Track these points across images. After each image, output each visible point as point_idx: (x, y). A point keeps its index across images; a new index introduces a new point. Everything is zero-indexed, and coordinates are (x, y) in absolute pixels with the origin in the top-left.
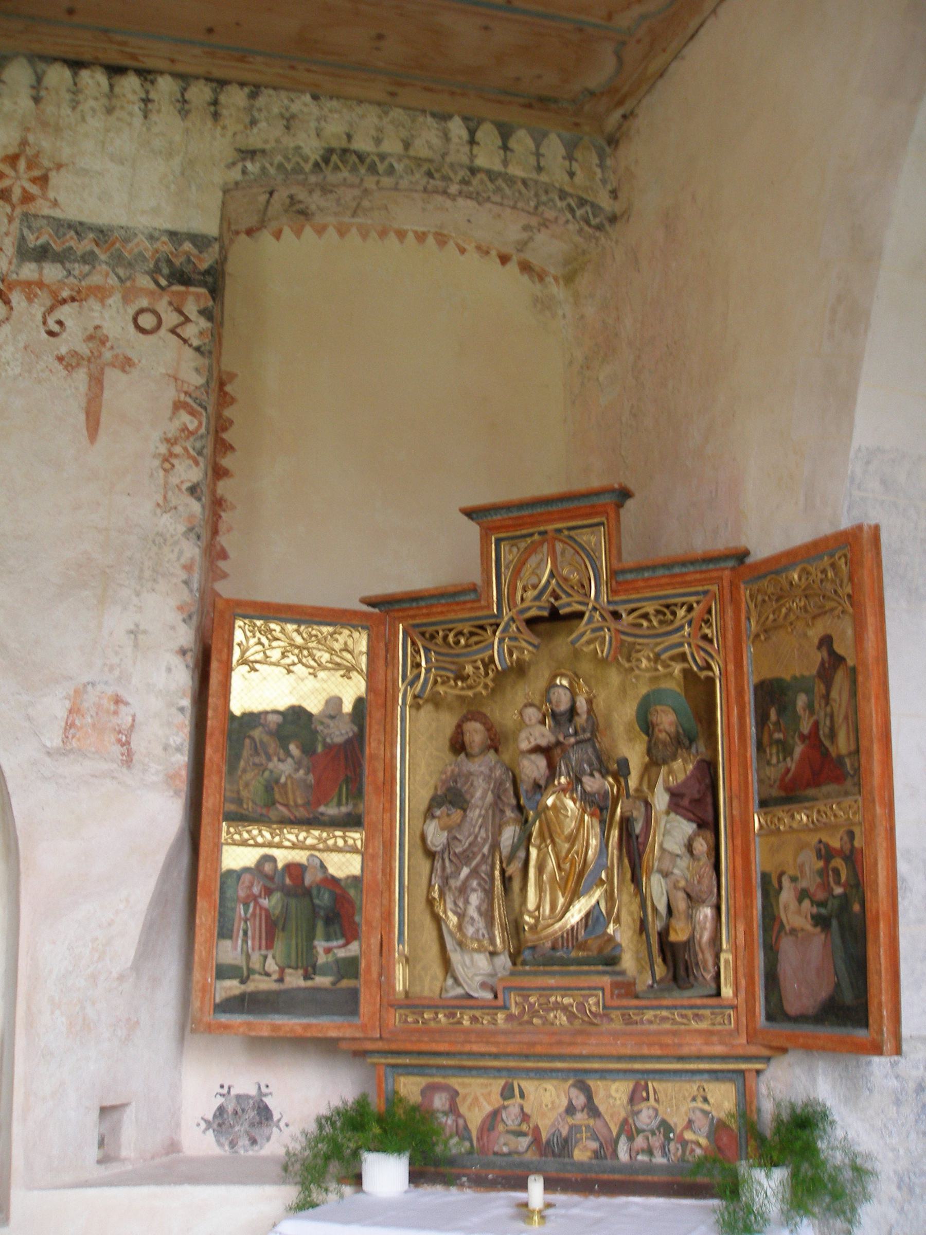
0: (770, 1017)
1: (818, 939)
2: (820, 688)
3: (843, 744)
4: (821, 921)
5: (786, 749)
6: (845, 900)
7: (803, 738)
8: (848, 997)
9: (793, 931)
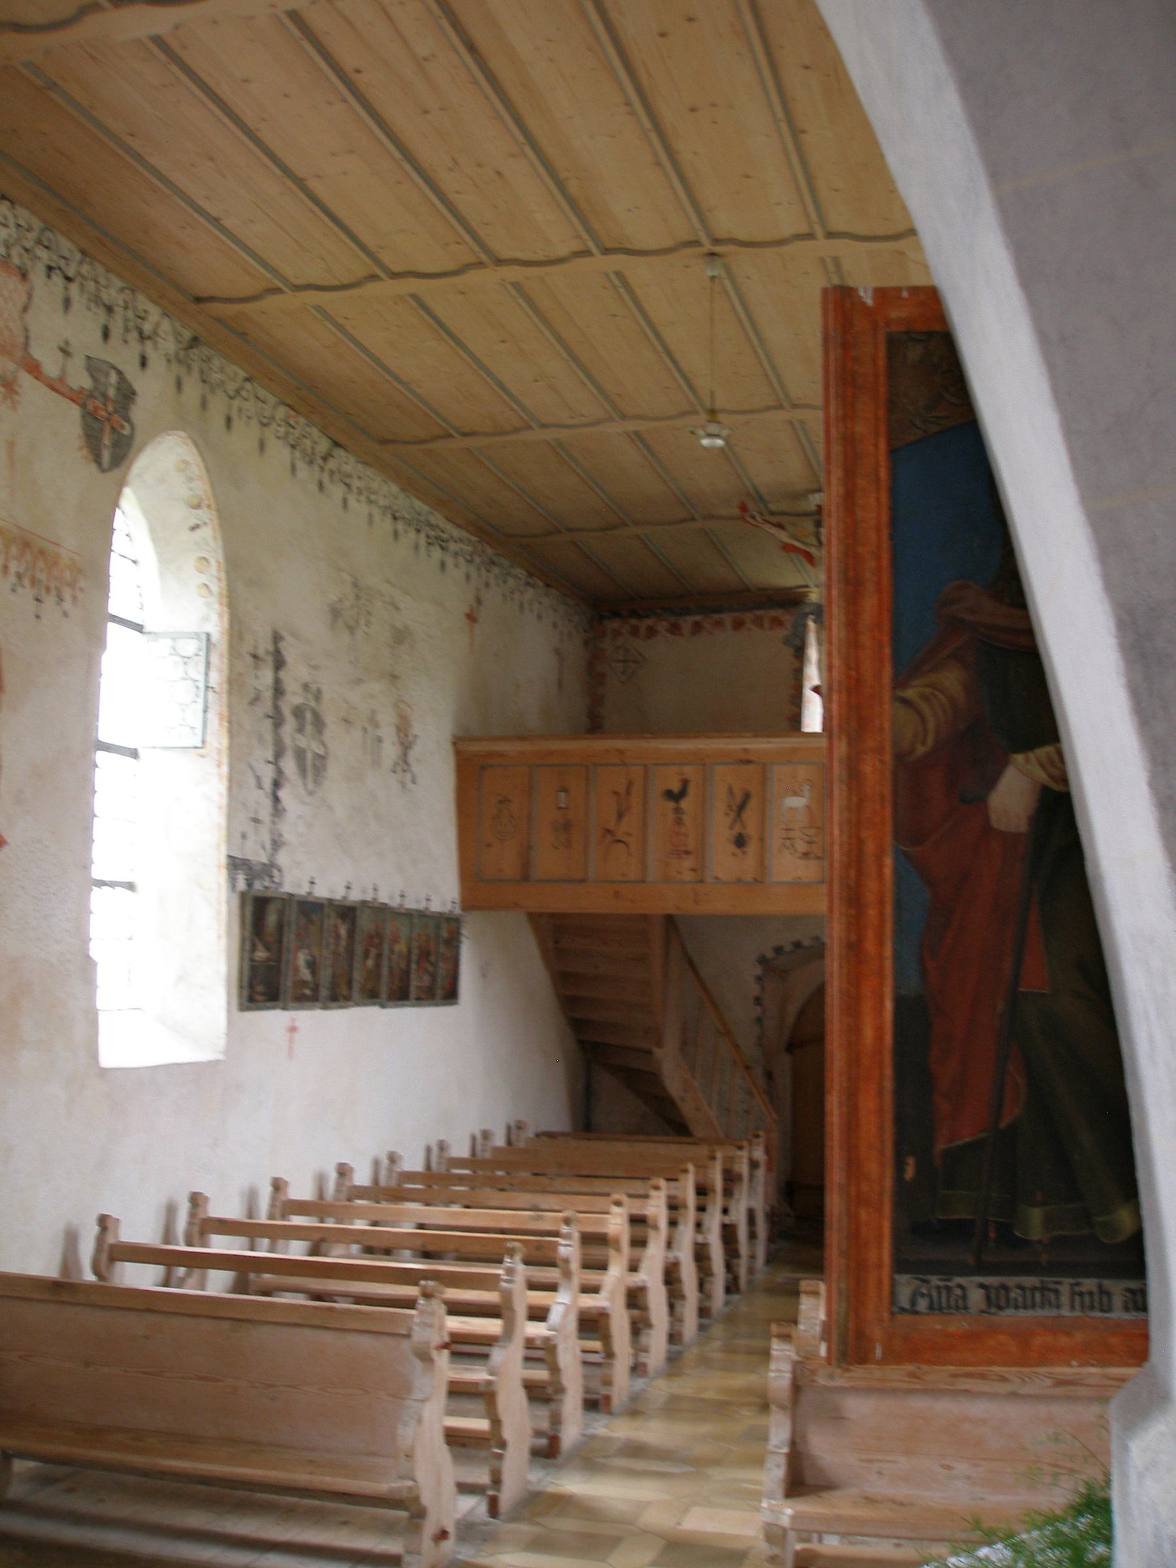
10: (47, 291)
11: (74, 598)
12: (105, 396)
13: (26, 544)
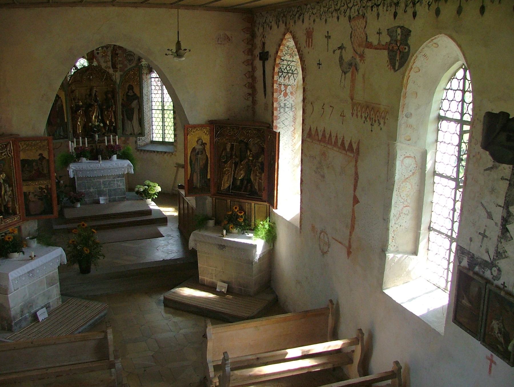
3: (45, 171)
4: (41, 200)
7: (35, 170)
9: (33, 201)
10: (370, 15)
11: (385, 123)
12: (396, 41)
13: (368, 107)
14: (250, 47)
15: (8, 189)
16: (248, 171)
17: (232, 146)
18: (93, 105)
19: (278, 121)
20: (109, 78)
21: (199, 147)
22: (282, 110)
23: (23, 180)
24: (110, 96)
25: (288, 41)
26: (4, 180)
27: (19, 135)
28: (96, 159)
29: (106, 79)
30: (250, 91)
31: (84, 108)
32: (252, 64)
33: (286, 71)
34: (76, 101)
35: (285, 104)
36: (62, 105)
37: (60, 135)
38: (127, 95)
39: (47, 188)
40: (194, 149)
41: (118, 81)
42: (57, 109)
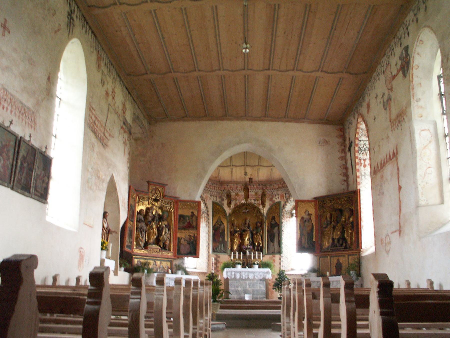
0: (178, 254)
1: (188, 246)
2: (191, 217)
4: (189, 244)
5: (184, 223)
6: (193, 242)
8: (192, 252)
14: (343, 147)
15: (167, 232)
16: (343, 233)
17: (331, 215)
18: (246, 230)
19: (361, 185)
20: (259, 211)
21: (306, 217)
22: (363, 177)
23: (179, 229)
24: (259, 224)
25: (361, 124)
26: (166, 226)
27: (179, 198)
28: (246, 267)
29: (257, 212)
30: (345, 178)
31: (240, 233)
32: (345, 159)
33: (363, 149)
34: (235, 227)
35: (365, 173)
36: (224, 229)
37: (221, 250)
38: (271, 223)
39: (194, 237)
40: (302, 218)
41: (265, 215)
42: (221, 231)
